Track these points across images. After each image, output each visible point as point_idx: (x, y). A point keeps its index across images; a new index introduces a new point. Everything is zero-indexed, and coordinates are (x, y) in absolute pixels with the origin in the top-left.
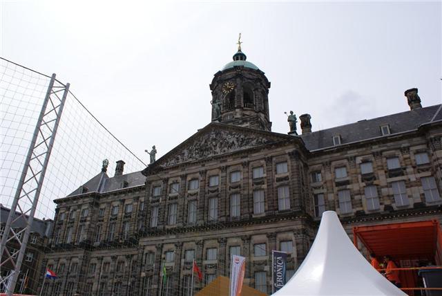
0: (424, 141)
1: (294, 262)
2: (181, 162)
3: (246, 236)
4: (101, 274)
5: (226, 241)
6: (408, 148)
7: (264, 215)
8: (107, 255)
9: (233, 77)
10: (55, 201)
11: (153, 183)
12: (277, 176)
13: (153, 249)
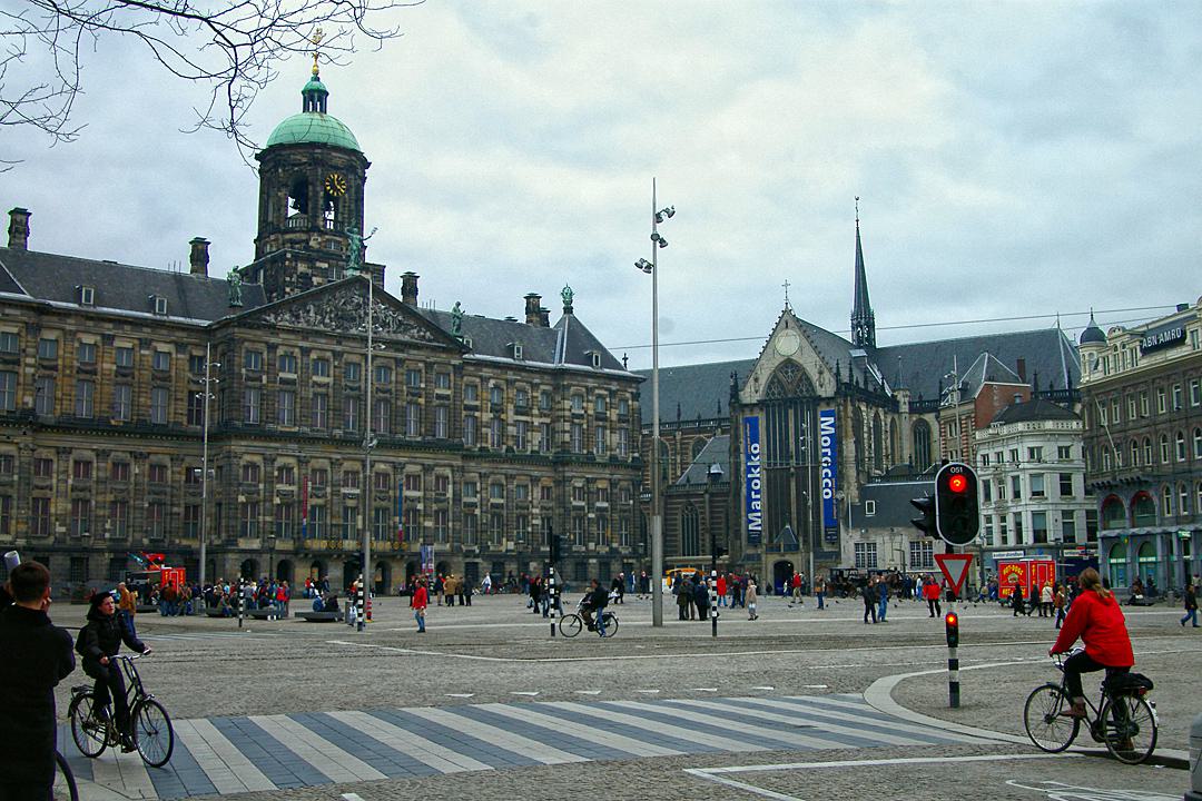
0: (552, 382)
2: (302, 325)
3: (400, 464)
4: (70, 481)
6: (537, 385)
7: (419, 439)
8: (85, 448)
11: (246, 344)
12: (437, 391)
13: (257, 459)
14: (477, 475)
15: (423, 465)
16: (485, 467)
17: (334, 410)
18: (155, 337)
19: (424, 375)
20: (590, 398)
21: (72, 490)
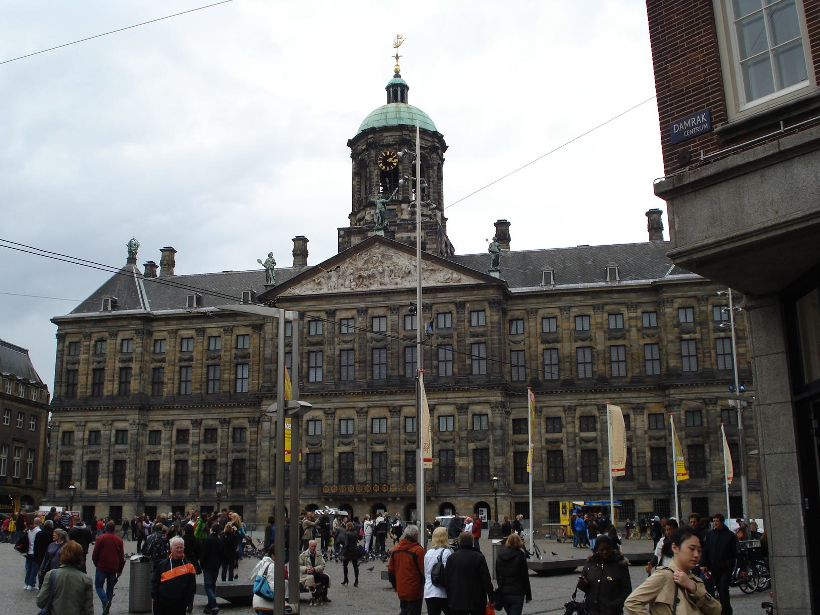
0: (654, 299)
1: (489, 441)
2: (324, 291)
5: (400, 411)
9: (397, 143)
10: (55, 321)
14: (561, 409)
15: (455, 404)
16: (569, 400)
17: (360, 362)
18: (234, 323)
19: (455, 315)
20: (703, 308)
21: (175, 453)
